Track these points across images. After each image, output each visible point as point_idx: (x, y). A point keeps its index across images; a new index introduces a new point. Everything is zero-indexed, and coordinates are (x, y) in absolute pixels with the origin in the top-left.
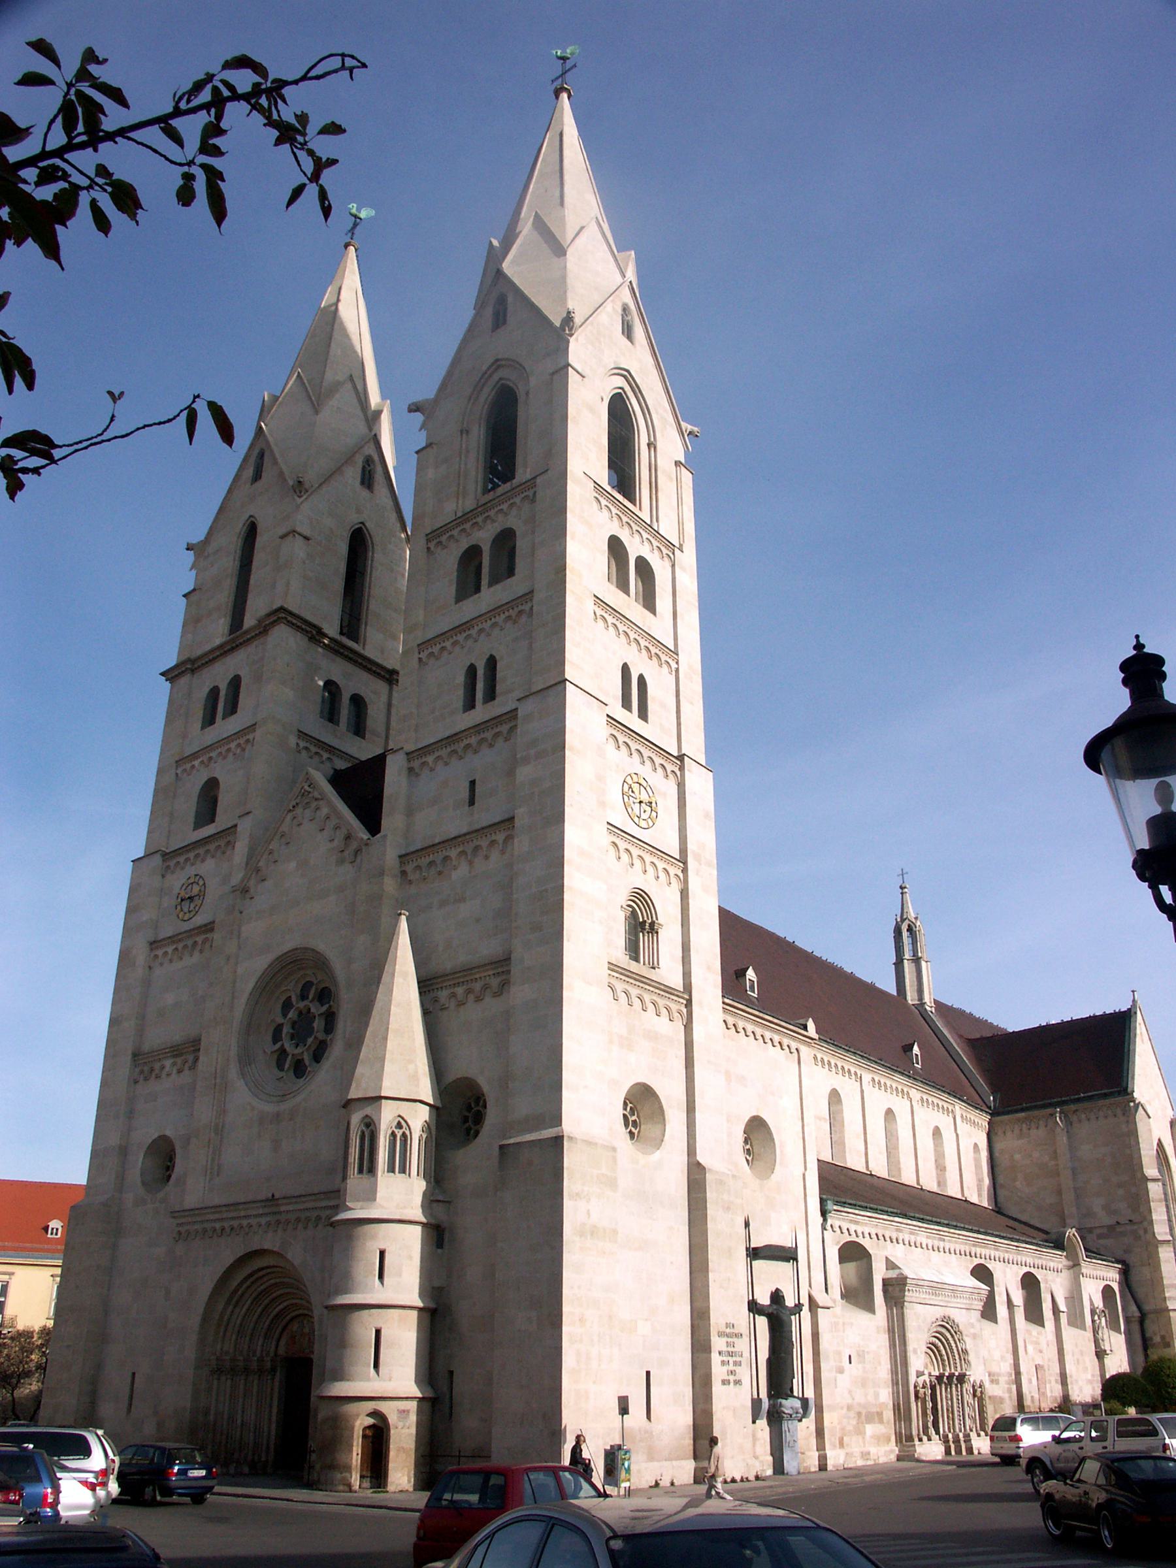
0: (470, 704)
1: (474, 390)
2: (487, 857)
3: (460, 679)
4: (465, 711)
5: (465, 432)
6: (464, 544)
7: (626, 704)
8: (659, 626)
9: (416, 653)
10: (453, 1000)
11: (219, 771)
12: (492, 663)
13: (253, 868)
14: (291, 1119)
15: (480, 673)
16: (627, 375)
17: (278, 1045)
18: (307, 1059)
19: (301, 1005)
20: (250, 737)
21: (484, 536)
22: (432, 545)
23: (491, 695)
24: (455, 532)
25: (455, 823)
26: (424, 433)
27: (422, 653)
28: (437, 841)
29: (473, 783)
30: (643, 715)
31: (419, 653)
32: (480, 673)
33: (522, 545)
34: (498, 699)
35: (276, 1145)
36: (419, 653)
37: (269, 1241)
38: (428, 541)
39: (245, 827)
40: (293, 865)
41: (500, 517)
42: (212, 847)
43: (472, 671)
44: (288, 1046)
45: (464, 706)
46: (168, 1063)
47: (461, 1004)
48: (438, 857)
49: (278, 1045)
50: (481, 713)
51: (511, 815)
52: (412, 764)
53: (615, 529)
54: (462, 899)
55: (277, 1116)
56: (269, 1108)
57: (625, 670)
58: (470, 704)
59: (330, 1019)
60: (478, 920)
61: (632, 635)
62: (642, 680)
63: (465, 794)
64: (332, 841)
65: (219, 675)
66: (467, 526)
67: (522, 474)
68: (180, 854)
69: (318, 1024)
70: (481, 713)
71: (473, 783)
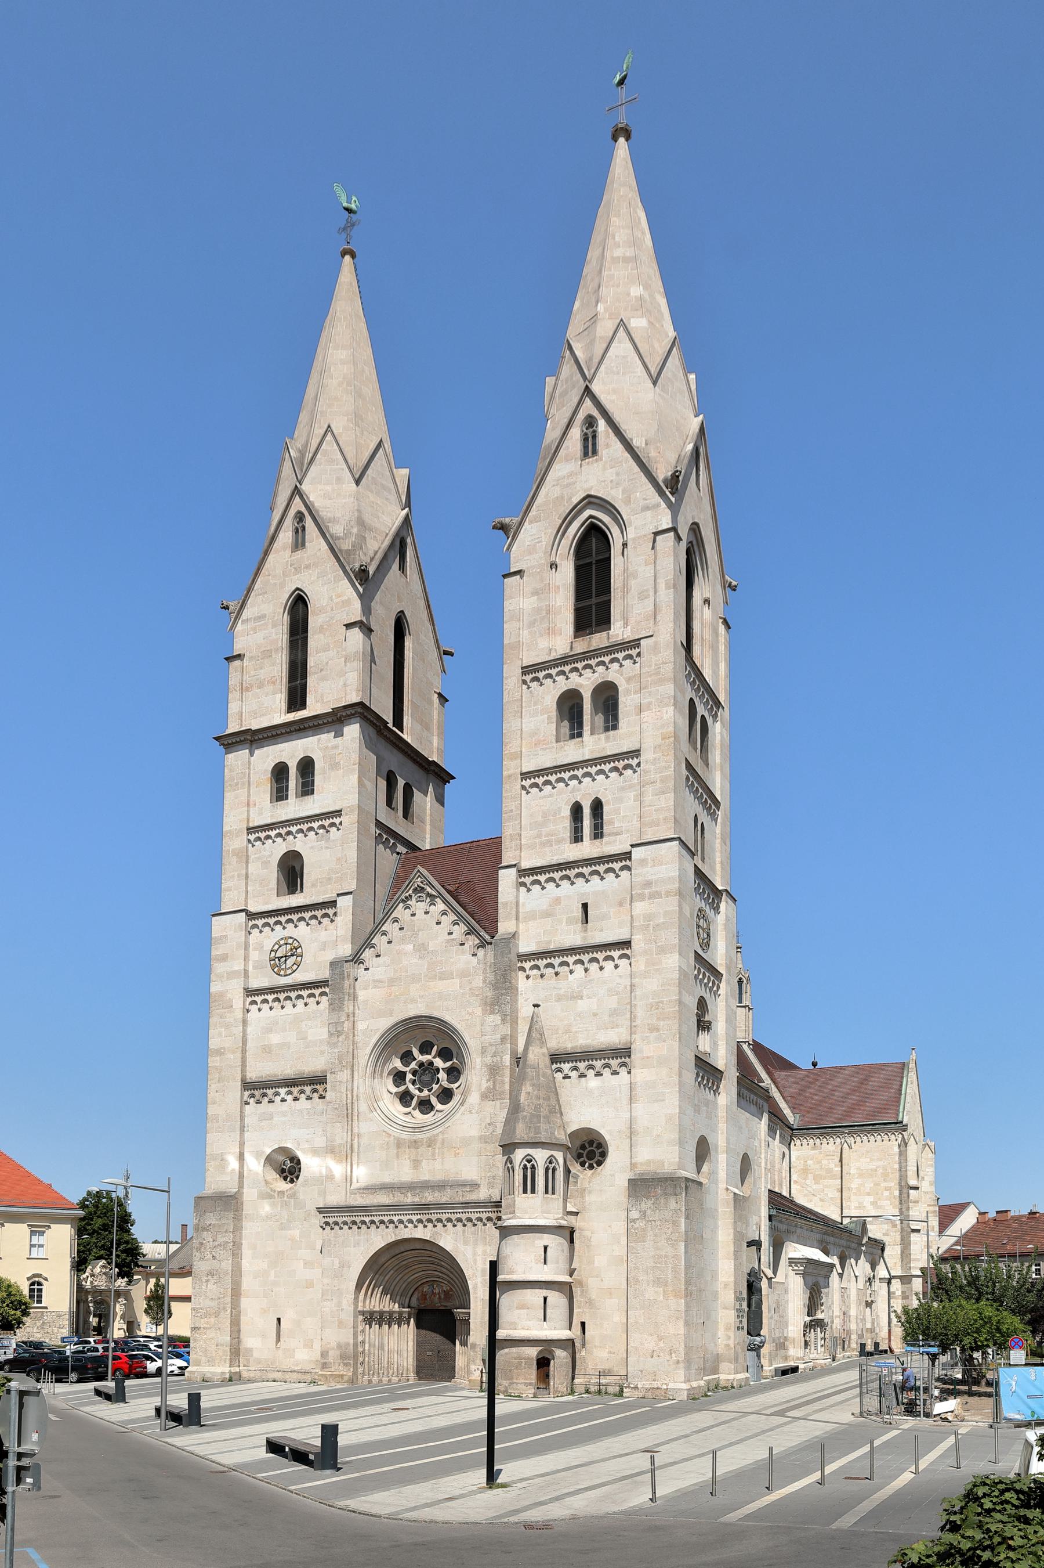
1: (563, 522)
2: (601, 968)
3: (567, 812)
6: (562, 685)
9: (520, 780)
10: (575, 1072)
11: (299, 844)
12: (597, 806)
13: (363, 943)
14: (429, 1146)
15: (587, 812)
17: (403, 1088)
18: (434, 1100)
19: (425, 1058)
20: (337, 821)
21: (586, 682)
22: (528, 678)
23: (598, 833)
24: (553, 672)
25: (573, 937)
27: (524, 781)
28: (552, 947)
29: (585, 906)
31: (522, 780)
32: (587, 812)
33: (626, 702)
34: (605, 839)
35: (416, 1164)
36: (522, 780)
37: (420, 1233)
38: (524, 673)
39: (345, 904)
40: (410, 947)
41: (601, 669)
42: (307, 915)
43: (577, 810)
44: (411, 1088)
46: (283, 1091)
47: (582, 1076)
48: (556, 961)
49: (403, 1088)
52: (523, 880)
53: (693, 695)
54: (582, 998)
55: (415, 1144)
56: (405, 1136)
58: (577, 838)
59: (454, 1073)
60: (595, 1015)
63: (579, 913)
64: (450, 934)
65: (291, 752)
66: (567, 668)
67: (619, 631)
68: (271, 916)
69: (442, 1076)
70: (588, 848)
71: (585, 906)
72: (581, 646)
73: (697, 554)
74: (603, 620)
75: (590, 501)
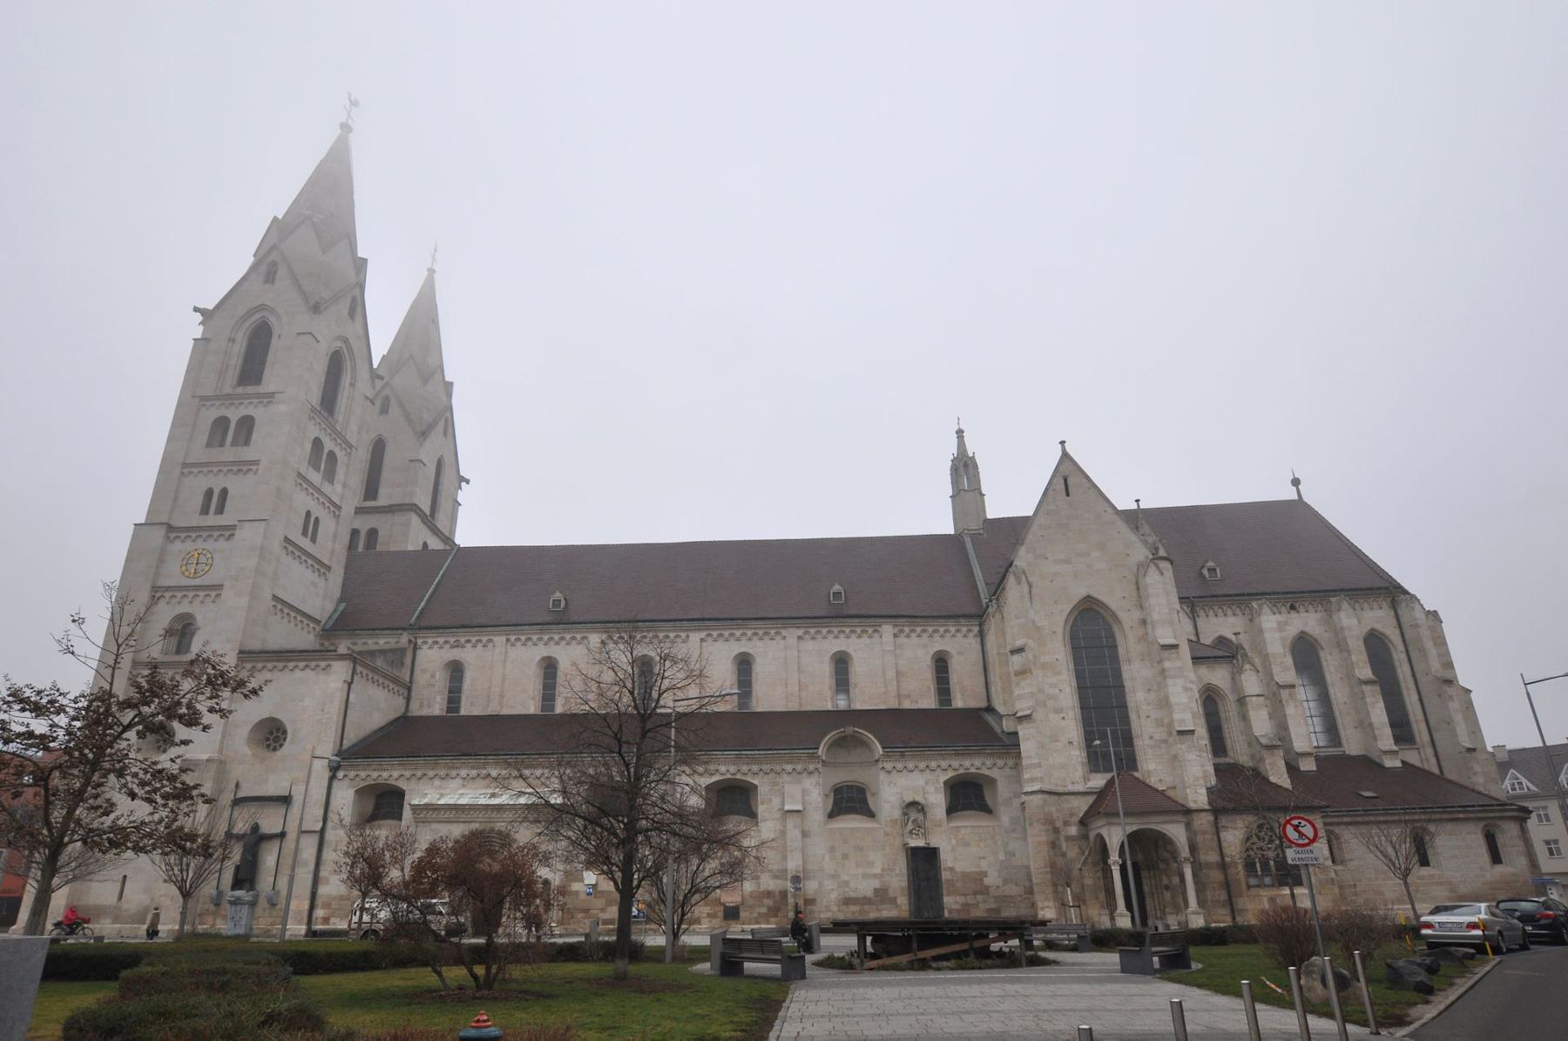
0: (205, 510)
4: (201, 514)
5: (232, 340)
6: (223, 412)
7: (305, 533)
8: (335, 491)
12: (224, 492)
16: (346, 341)
21: (234, 415)
23: (220, 510)
26: (201, 327)
30: (313, 540)
43: (209, 493)
45: (202, 510)
50: (212, 519)
51: (221, 583)
57: (308, 514)
61: (322, 500)
62: (317, 520)
70: (212, 519)
72: (240, 390)
73: (348, 363)
74: (258, 380)
75: (262, 307)
